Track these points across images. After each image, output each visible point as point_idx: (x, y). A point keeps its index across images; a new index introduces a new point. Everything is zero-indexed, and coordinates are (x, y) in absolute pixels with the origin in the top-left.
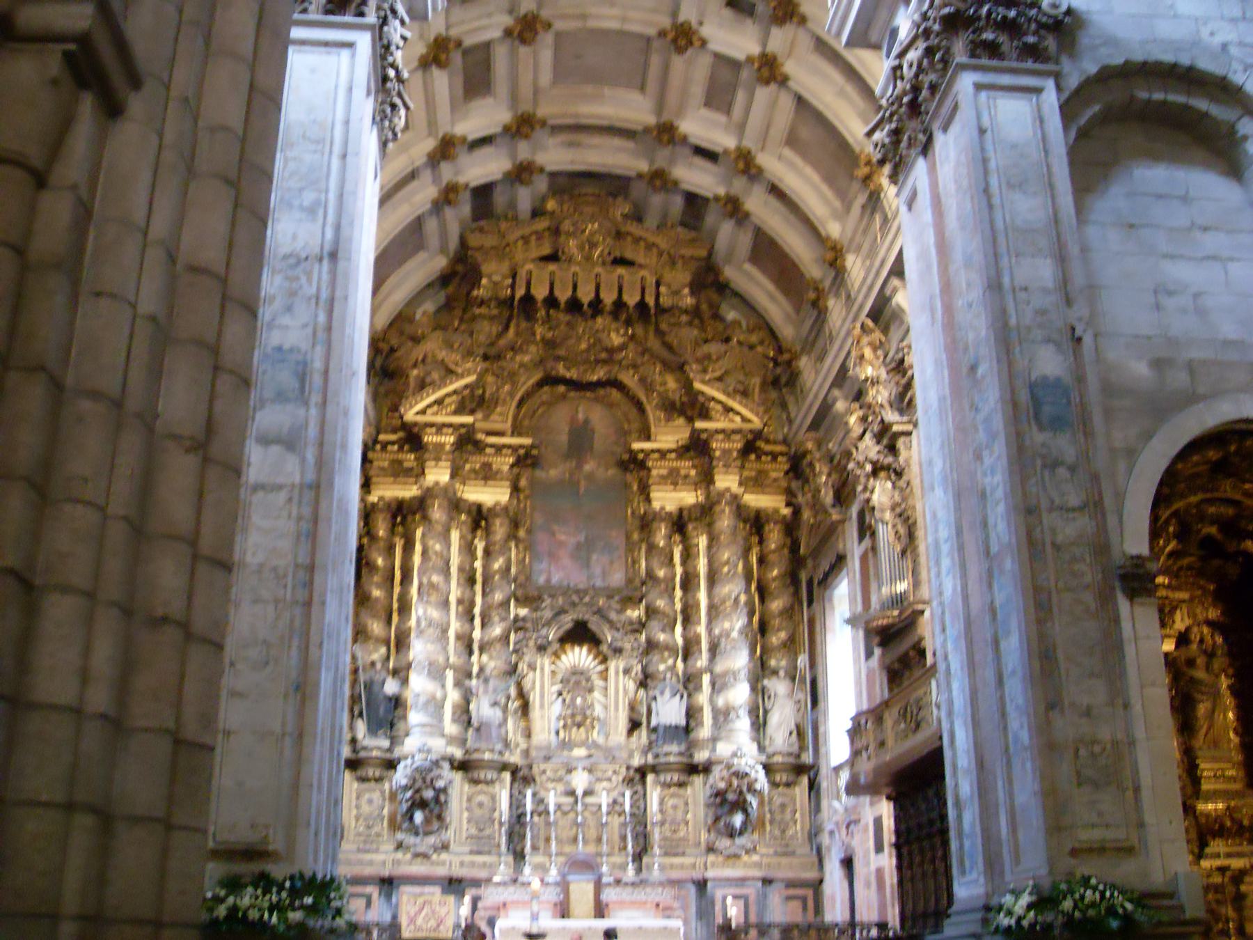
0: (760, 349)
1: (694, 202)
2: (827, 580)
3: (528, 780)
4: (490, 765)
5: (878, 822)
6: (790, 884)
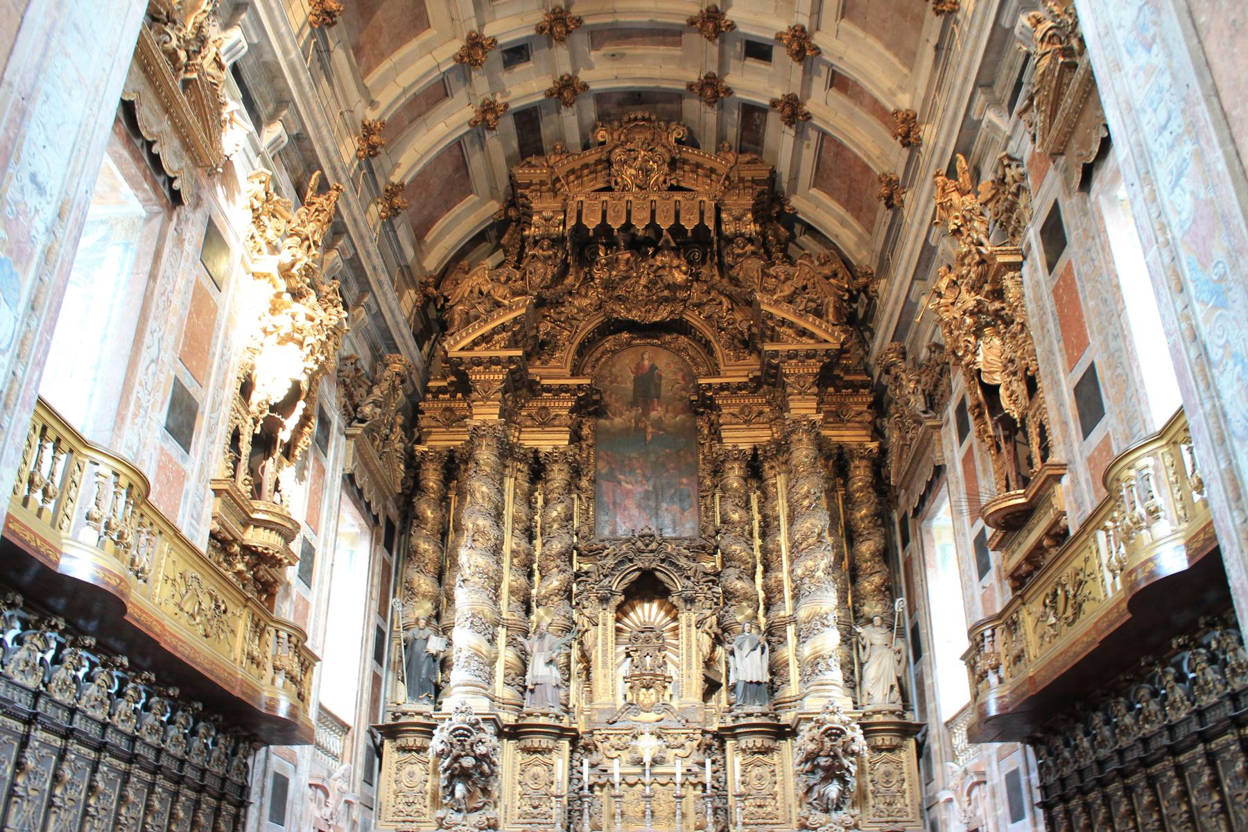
0: (832, 281)
1: (752, 114)
5: (1012, 780)
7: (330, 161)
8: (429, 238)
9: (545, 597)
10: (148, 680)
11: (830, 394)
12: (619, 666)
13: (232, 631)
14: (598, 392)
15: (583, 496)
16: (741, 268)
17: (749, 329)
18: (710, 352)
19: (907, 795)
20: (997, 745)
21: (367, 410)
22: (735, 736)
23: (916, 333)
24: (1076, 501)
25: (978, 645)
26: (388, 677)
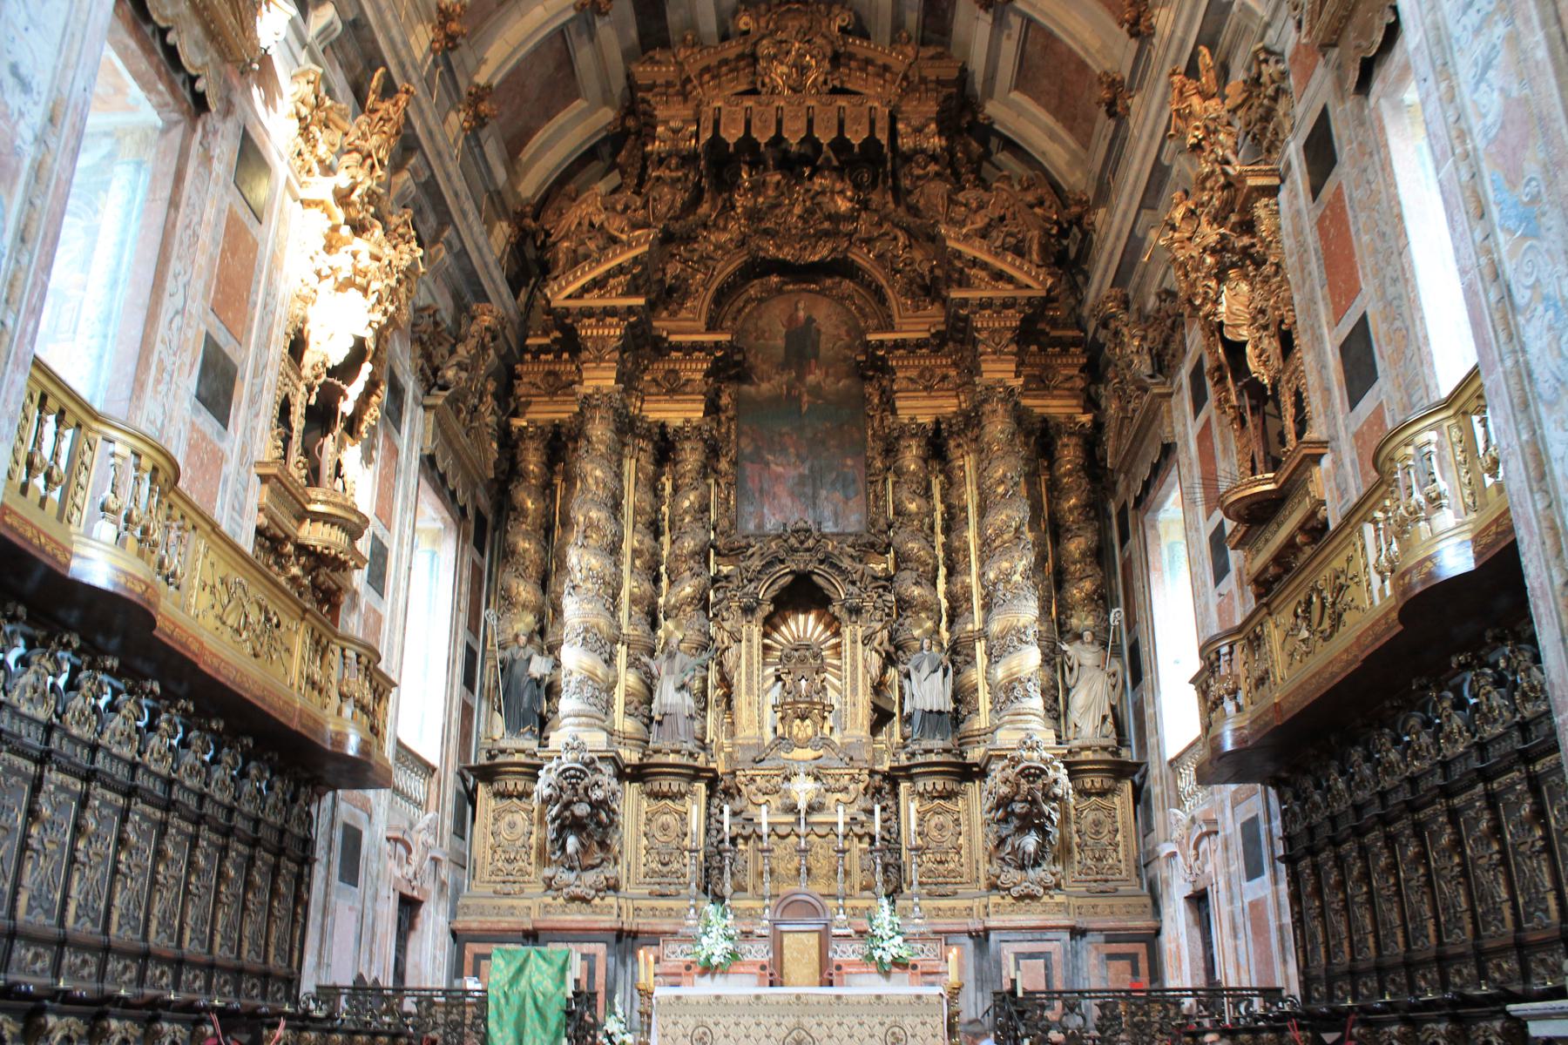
0: (1037, 210)
2: (1145, 499)
3: (730, 793)
4: (677, 771)
5: (1250, 830)
6: (1112, 937)
7: (397, 54)
8: (525, 156)
9: (674, 607)
10: (185, 710)
11: (1033, 354)
12: (767, 692)
13: (288, 650)
14: (740, 350)
15: (722, 483)
16: (922, 193)
17: (932, 270)
18: (882, 299)
19: (1121, 849)
20: (1233, 787)
21: (450, 374)
22: (910, 778)
23: (1142, 276)
24: (1338, 488)
25: (1211, 664)
26: (482, 708)
